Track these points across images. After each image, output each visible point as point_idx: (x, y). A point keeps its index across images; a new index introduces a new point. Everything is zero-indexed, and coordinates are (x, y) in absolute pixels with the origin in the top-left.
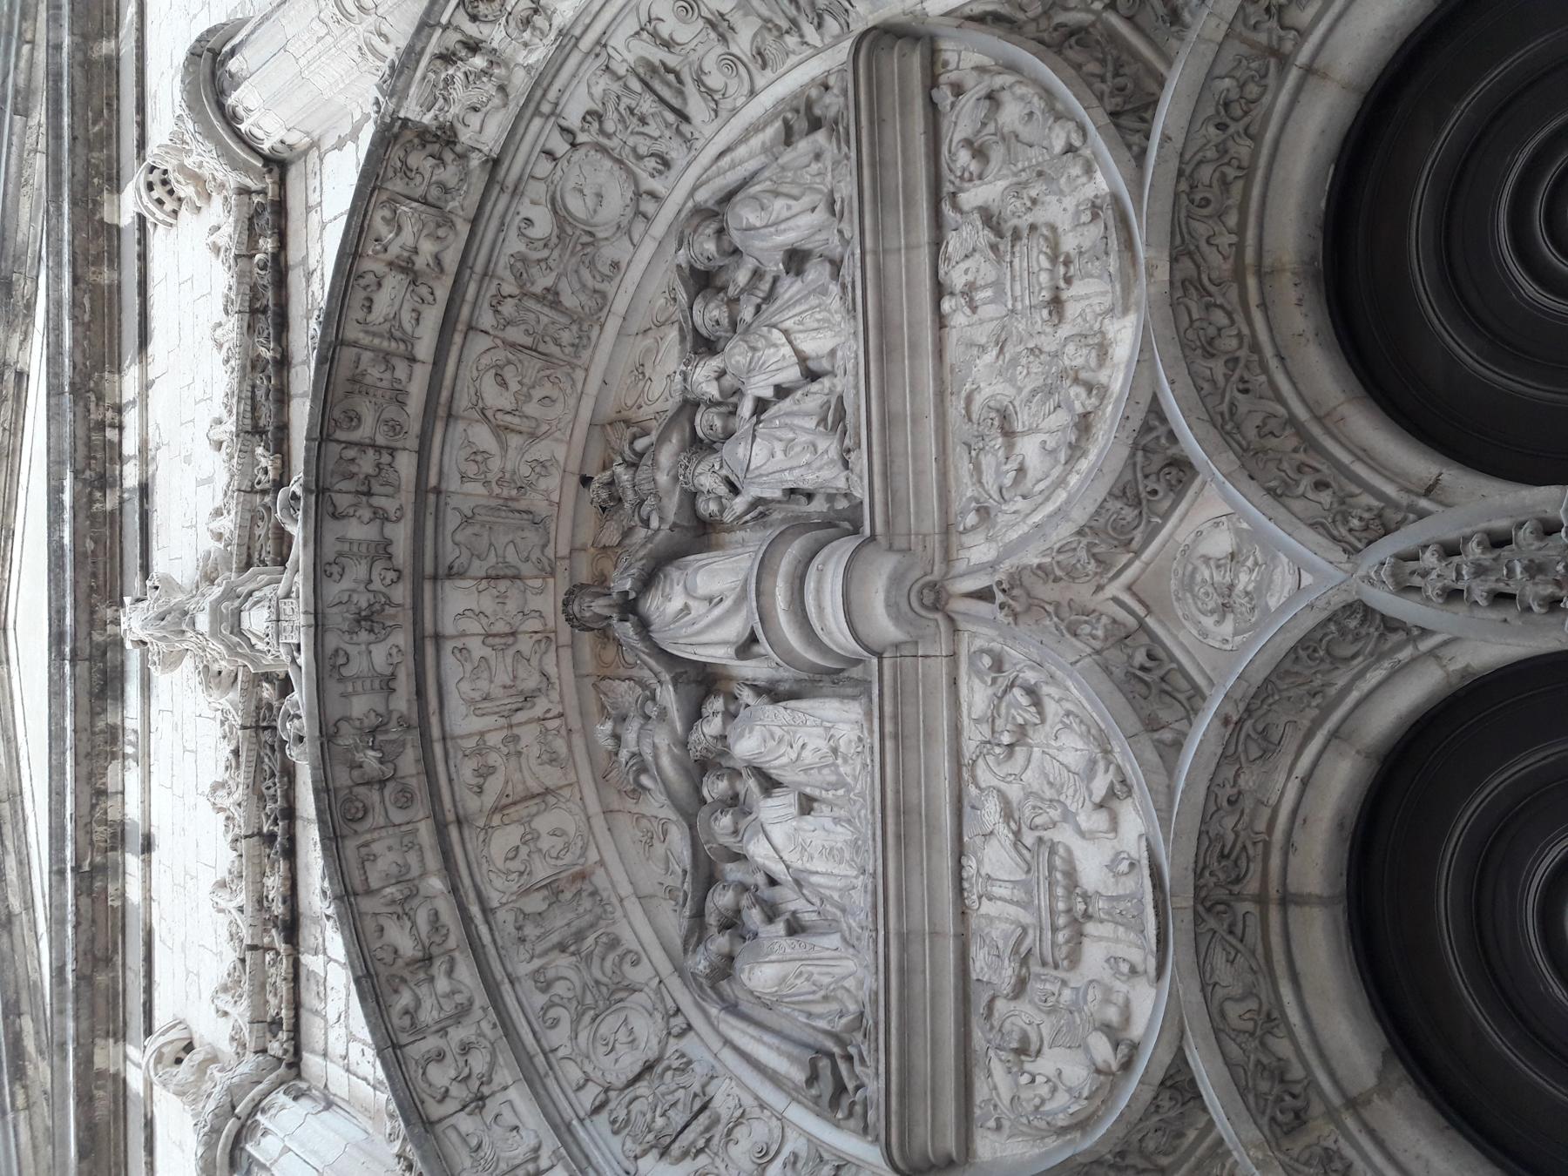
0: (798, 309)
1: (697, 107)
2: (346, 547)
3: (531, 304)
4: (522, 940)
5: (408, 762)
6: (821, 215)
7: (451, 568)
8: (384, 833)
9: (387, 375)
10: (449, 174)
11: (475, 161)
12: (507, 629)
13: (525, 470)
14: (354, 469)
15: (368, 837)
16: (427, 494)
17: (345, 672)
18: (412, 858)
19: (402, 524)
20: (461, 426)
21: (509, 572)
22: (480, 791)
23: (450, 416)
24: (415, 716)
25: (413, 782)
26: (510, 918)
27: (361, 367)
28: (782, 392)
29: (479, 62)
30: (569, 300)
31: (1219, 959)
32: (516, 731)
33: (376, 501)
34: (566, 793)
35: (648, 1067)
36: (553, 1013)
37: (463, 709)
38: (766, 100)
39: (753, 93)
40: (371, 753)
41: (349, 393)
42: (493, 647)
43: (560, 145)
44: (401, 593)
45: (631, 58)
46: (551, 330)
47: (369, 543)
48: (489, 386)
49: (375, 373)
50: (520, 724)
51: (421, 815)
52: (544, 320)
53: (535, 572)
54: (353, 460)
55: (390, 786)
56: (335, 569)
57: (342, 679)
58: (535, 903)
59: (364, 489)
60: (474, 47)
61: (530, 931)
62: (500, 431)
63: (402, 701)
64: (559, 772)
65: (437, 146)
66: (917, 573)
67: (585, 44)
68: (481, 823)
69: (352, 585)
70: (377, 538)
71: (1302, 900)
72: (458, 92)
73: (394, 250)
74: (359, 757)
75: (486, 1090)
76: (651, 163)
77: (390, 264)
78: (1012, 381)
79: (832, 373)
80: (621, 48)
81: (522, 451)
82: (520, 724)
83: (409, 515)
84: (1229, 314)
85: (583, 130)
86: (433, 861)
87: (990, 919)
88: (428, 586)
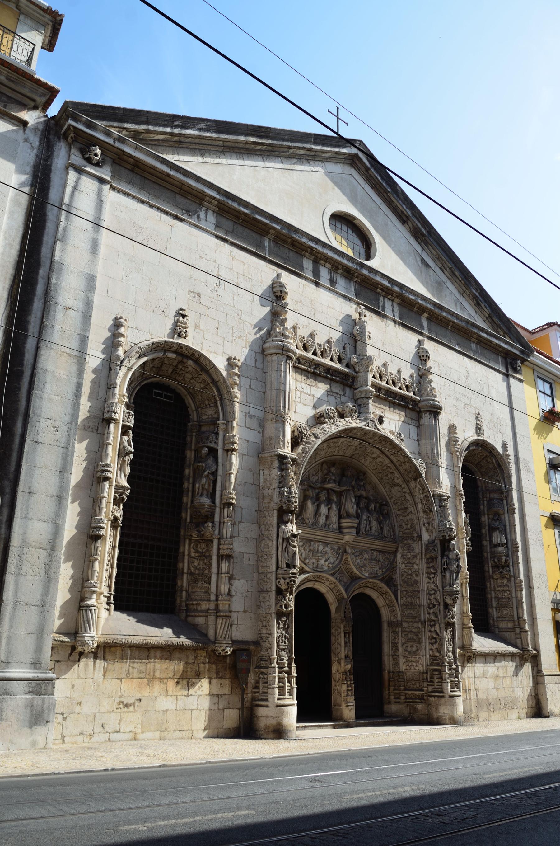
1: (399, 513)
6: (386, 535)
10: (410, 476)
28: (370, 521)
29: (421, 492)
43: (404, 490)
48: (381, 460)
60: (423, 493)
62: (374, 458)
71: (314, 584)
72: (418, 486)
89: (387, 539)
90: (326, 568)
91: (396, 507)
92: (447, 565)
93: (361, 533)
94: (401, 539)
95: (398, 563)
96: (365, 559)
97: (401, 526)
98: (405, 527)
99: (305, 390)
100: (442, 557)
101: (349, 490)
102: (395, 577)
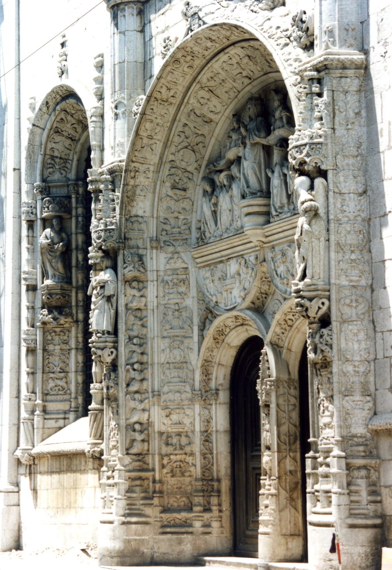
75: (154, 137)
86: (186, 84)
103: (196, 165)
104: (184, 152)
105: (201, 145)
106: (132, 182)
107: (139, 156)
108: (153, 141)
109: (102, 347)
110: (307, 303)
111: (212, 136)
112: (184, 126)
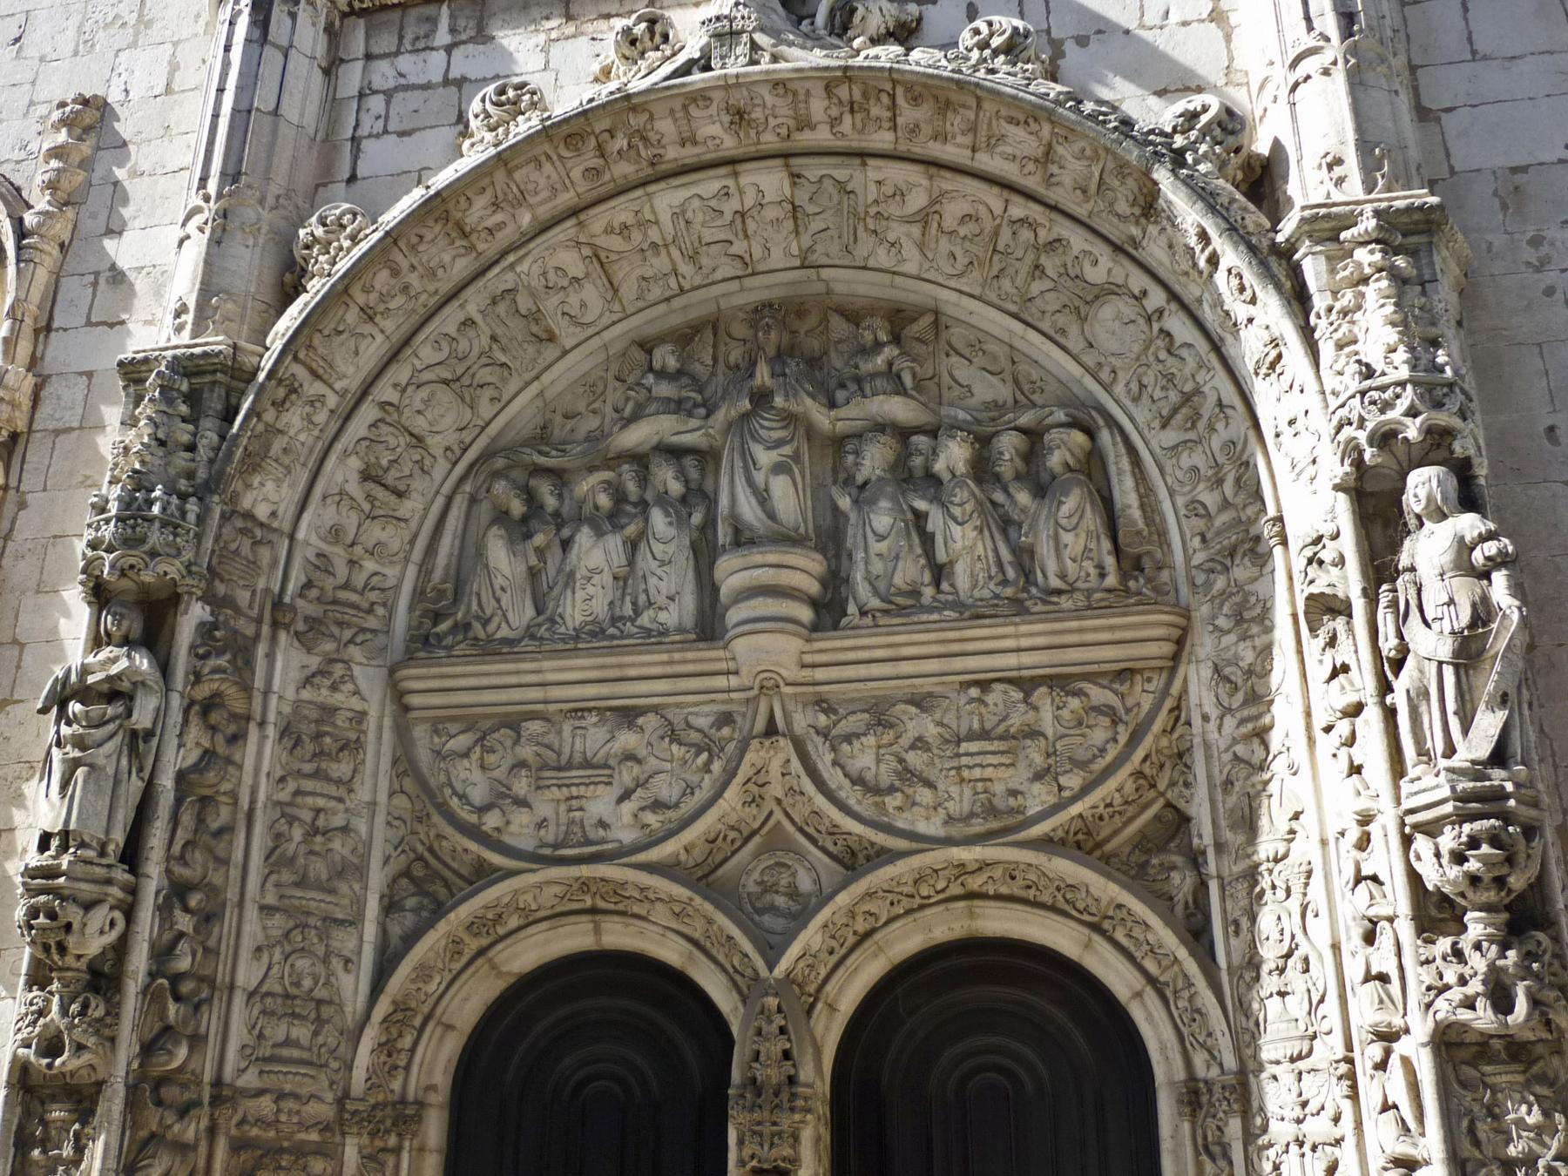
0: (991, 554)
2: (802, 98)
3: (1030, 257)
4: (494, 302)
5: (623, 170)
7: (799, 176)
8: (560, 168)
9: (957, 130)
11: (1135, 231)
12: (750, 232)
13: (891, 237)
14: (872, 102)
15: (555, 158)
16: (863, 155)
17: (693, 111)
18: (545, 194)
19: (830, 136)
20: (925, 182)
21: (801, 229)
22: (609, 230)
23: (931, 178)
24: (663, 167)
25: (607, 177)
26: (509, 286)
27: (961, 110)
30: (1036, 287)
31: (557, 889)
32: (663, 252)
33: (847, 119)
34: (617, 307)
35: (420, 439)
36: (445, 344)
37: (676, 202)
38: (1167, 506)
39: (1172, 492)
40: (625, 143)
41: (937, 99)
42: (733, 222)
44: (770, 141)
45: (1206, 389)
46: (1010, 270)
47: (809, 115)
49: (955, 122)
50: (669, 254)
51: (580, 190)
52: (1018, 264)
53: (804, 247)
54: (878, 99)
55: (598, 162)
56: (781, 91)
57: (685, 107)
58: (524, 303)
59: (856, 107)
61: (502, 308)
62: (923, 218)
63: (674, 154)
64: (632, 297)
65: (1141, 200)
66: (784, 673)
67: (1214, 360)
68: (582, 239)
69: (769, 105)
70: (814, 120)
71: (597, 931)
73: (1060, 150)
74: (620, 135)
75: (378, 319)
76: (1134, 386)
77: (1050, 145)
78: (913, 747)
79: (939, 591)
80: (1213, 383)
81: (908, 235)
82: (669, 254)
83: (840, 144)
84: (943, 890)
85: (1161, 330)
86: (544, 212)
87: (559, 733)
88: (779, 162)
89: (1065, 602)
90: (628, 836)
91: (1142, 414)
92: (1400, 636)
93: (852, 608)
94: (1200, 578)
95: (1197, 721)
96: (919, 743)
97: (1196, 508)
98: (1210, 499)
99: (412, 80)
100: (1371, 598)
101: (745, 416)
102: (1192, 811)
103: (451, 438)
104: (433, 394)
105: (487, 393)
106: (269, 416)
107: (320, 350)
108: (368, 328)
109: (87, 897)
110: (73, 914)
111: (537, 378)
112: (464, 323)
